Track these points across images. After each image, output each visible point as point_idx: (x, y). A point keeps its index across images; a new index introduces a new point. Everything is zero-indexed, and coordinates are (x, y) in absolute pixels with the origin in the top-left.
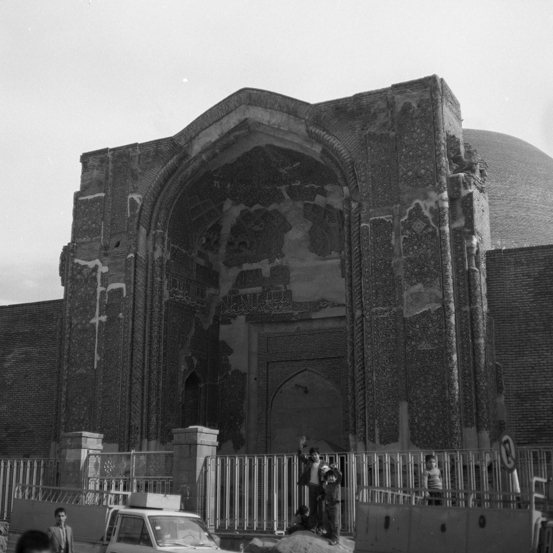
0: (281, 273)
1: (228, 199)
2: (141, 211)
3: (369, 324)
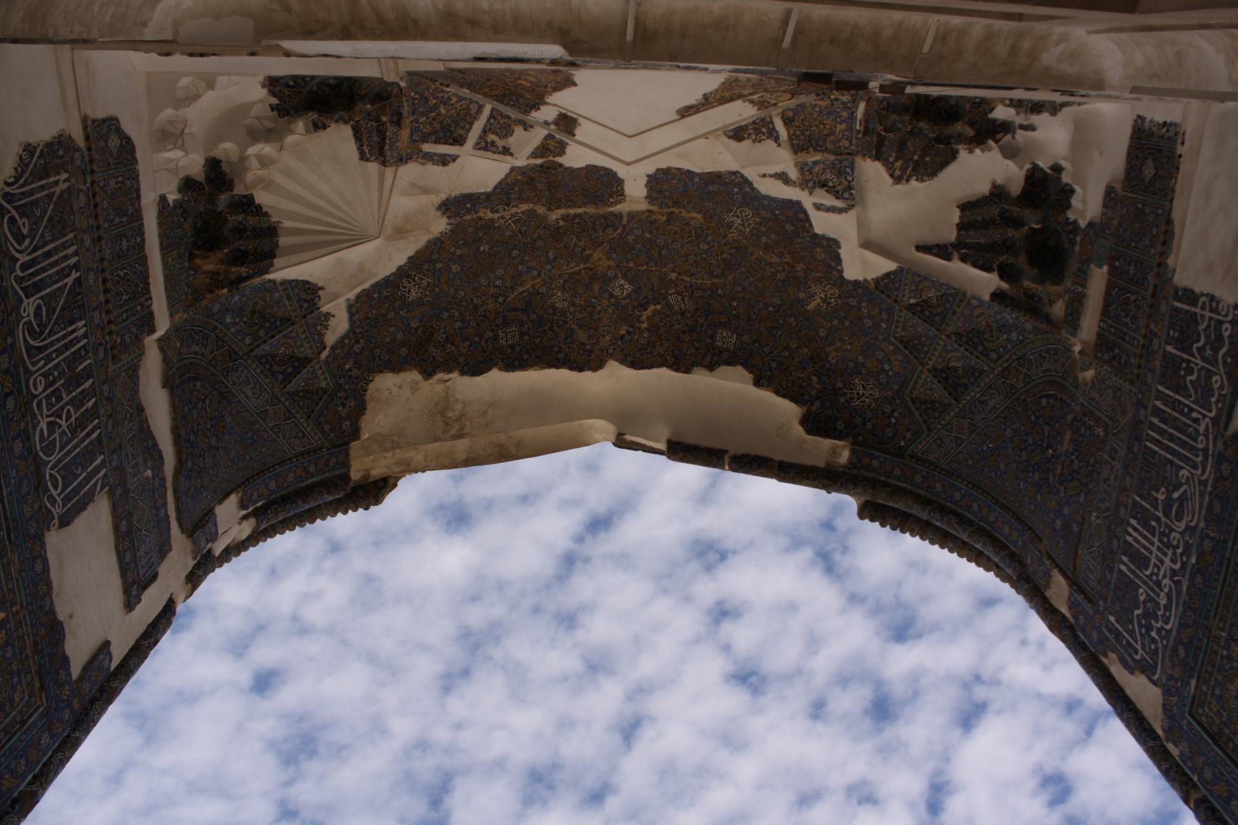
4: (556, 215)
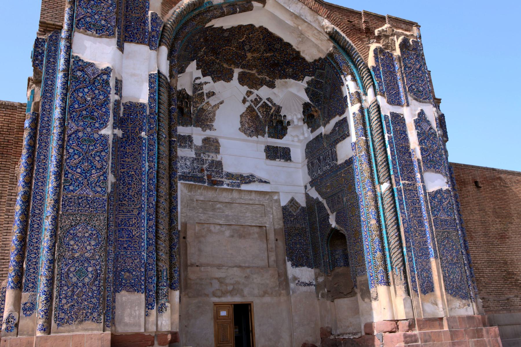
0: (212, 145)
1: (195, 61)
2: (163, 31)
4: (254, 72)
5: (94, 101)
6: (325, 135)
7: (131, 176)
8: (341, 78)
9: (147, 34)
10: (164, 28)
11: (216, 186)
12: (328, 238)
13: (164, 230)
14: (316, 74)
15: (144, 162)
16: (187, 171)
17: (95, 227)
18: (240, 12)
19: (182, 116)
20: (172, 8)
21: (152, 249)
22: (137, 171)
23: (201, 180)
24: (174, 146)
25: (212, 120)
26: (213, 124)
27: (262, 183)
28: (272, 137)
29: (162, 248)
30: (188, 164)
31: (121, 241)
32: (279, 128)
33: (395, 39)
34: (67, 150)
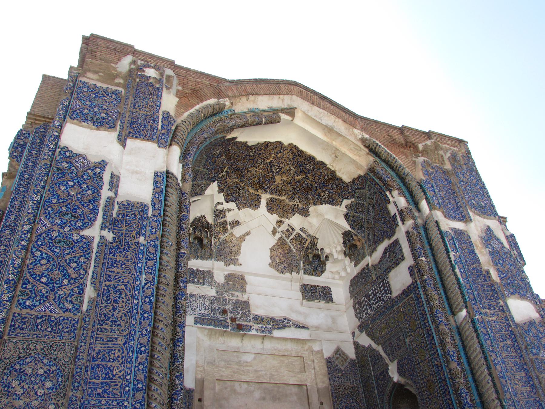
0: (236, 282)
1: (217, 182)
2: (175, 131)
3: (482, 325)
5: (79, 195)
6: (372, 265)
7: (120, 292)
8: (386, 195)
9: (155, 131)
10: (176, 128)
11: (241, 332)
12: (390, 396)
13: (162, 369)
14: (357, 194)
15: (139, 274)
16: (206, 312)
17: (55, 359)
18: (266, 123)
19: (202, 248)
20: (187, 111)
21: (140, 397)
22: (129, 286)
23: (221, 324)
24: (183, 259)
25: (237, 253)
26: (239, 258)
27: (299, 329)
28: (309, 274)
29: (157, 396)
30: (207, 304)
31: (94, 383)
32: (316, 262)
33: (443, 154)
34: (32, 252)
